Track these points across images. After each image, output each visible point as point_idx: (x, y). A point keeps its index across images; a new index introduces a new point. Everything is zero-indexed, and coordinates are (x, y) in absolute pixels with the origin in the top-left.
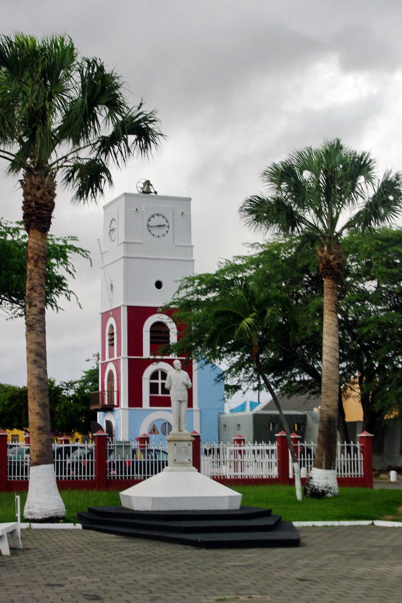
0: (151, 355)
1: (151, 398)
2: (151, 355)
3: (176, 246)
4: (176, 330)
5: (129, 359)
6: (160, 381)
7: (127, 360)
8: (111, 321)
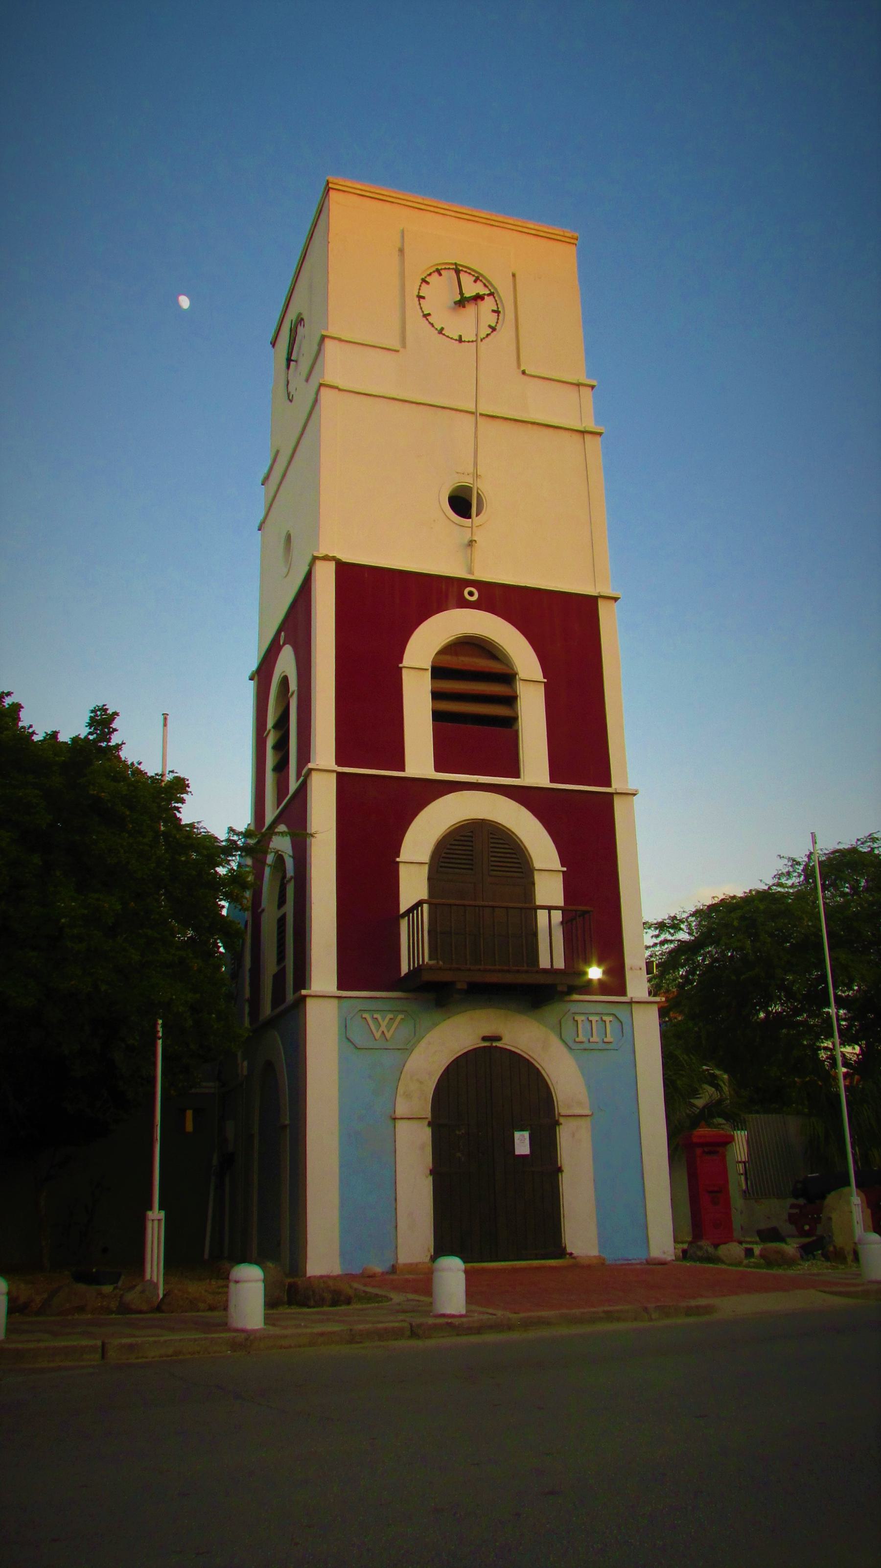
0: (439, 766)
2: (438, 768)
4: (538, 675)
7: (331, 781)
8: (286, 663)
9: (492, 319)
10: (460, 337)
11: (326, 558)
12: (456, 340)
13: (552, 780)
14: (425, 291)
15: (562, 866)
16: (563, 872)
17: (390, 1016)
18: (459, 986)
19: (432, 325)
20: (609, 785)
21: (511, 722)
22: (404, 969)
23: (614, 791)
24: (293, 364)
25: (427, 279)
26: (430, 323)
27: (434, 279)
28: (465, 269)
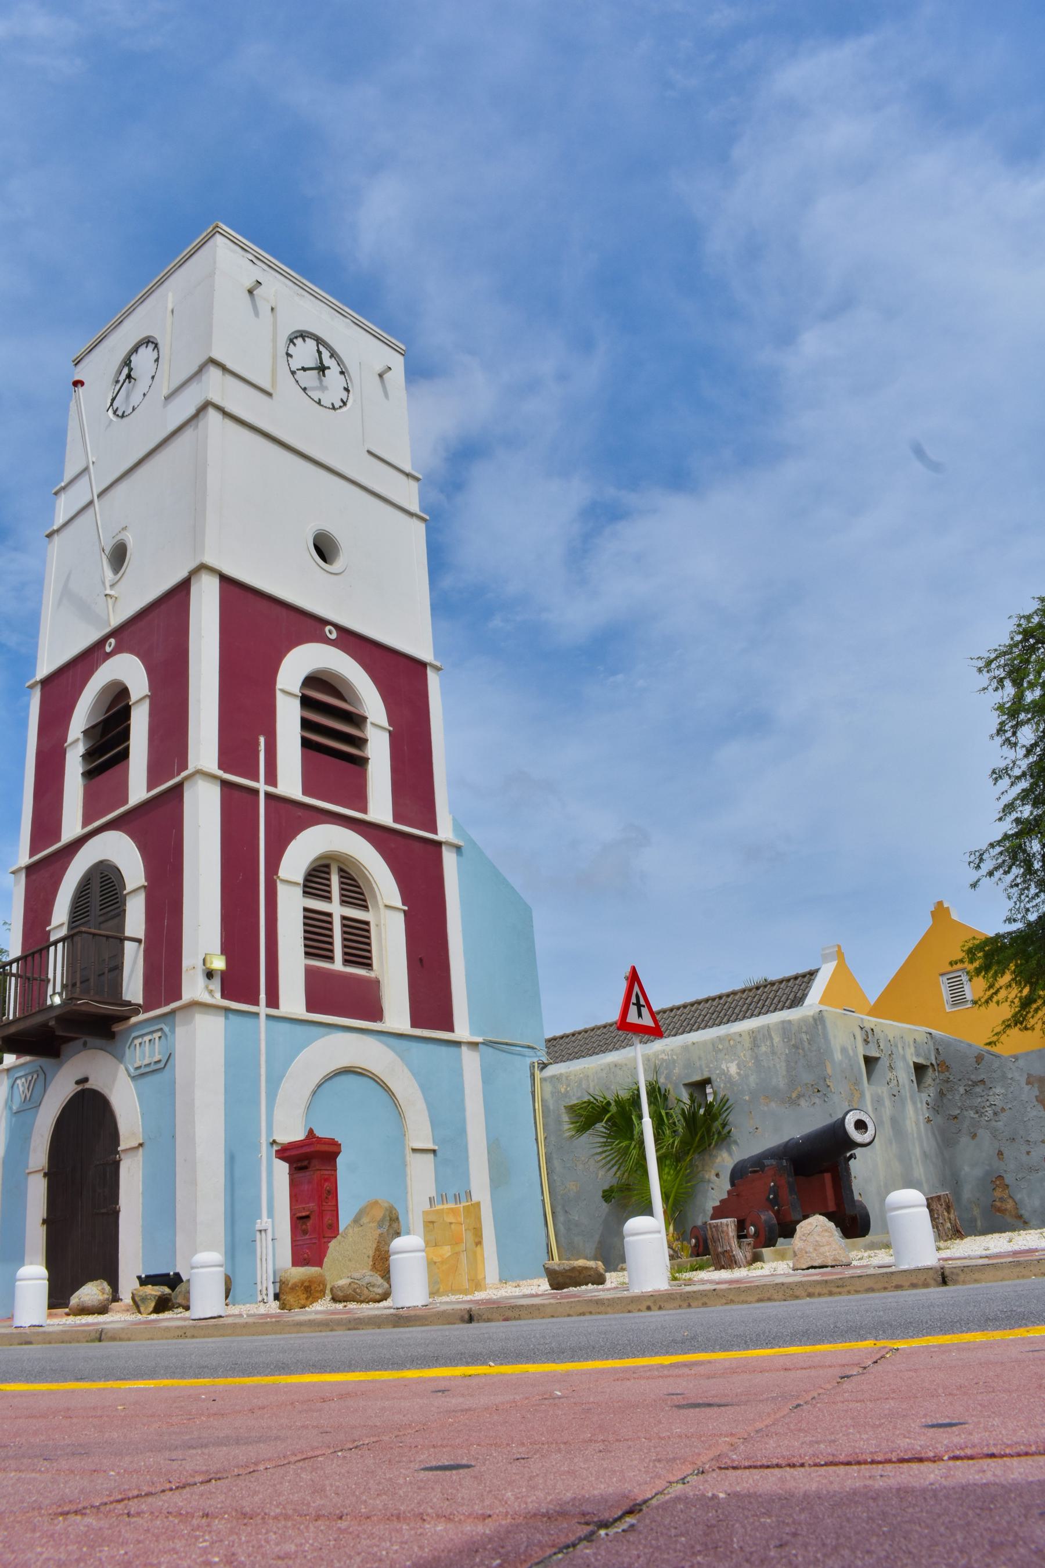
1: (310, 972)
3: (369, 452)
5: (225, 784)
6: (336, 909)
10: (320, 400)
11: (212, 570)
14: (292, 350)
15: (404, 904)
16: (404, 911)
21: (362, 762)
25: (295, 341)
27: (299, 341)
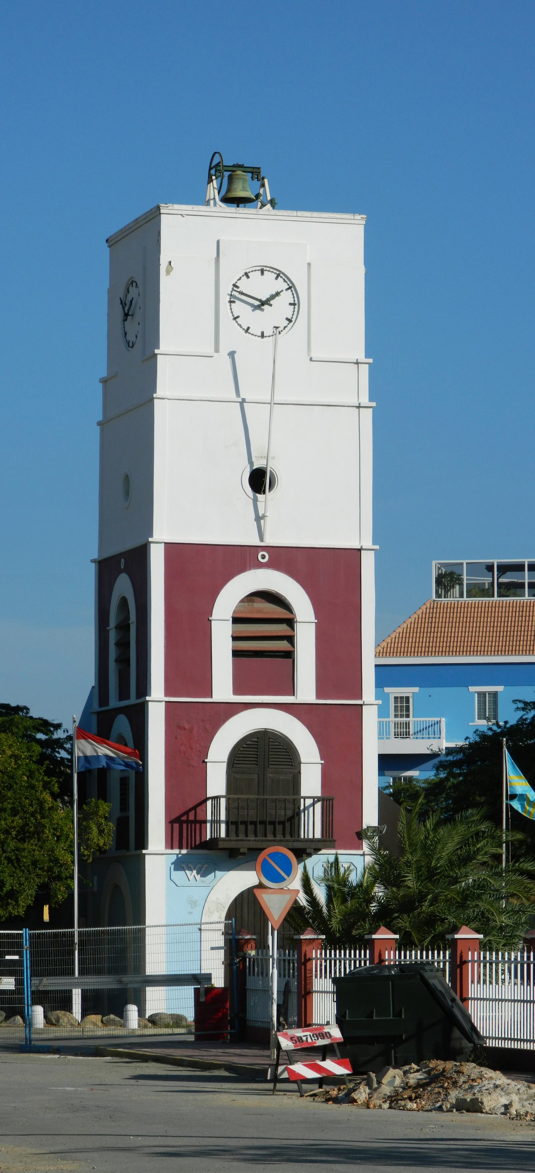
7: (162, 706)
9: (289, 311)
12: (259, 336)
13: (318, 696)
17: (200, 866)
18: (242, 851)
19: (240, 326)
20: (360, 697)
21: (289, 655)
22: (208, 837)
23: (362, 703)
24: (129, 318)
26: (239, 324)
28: (268, 269)
